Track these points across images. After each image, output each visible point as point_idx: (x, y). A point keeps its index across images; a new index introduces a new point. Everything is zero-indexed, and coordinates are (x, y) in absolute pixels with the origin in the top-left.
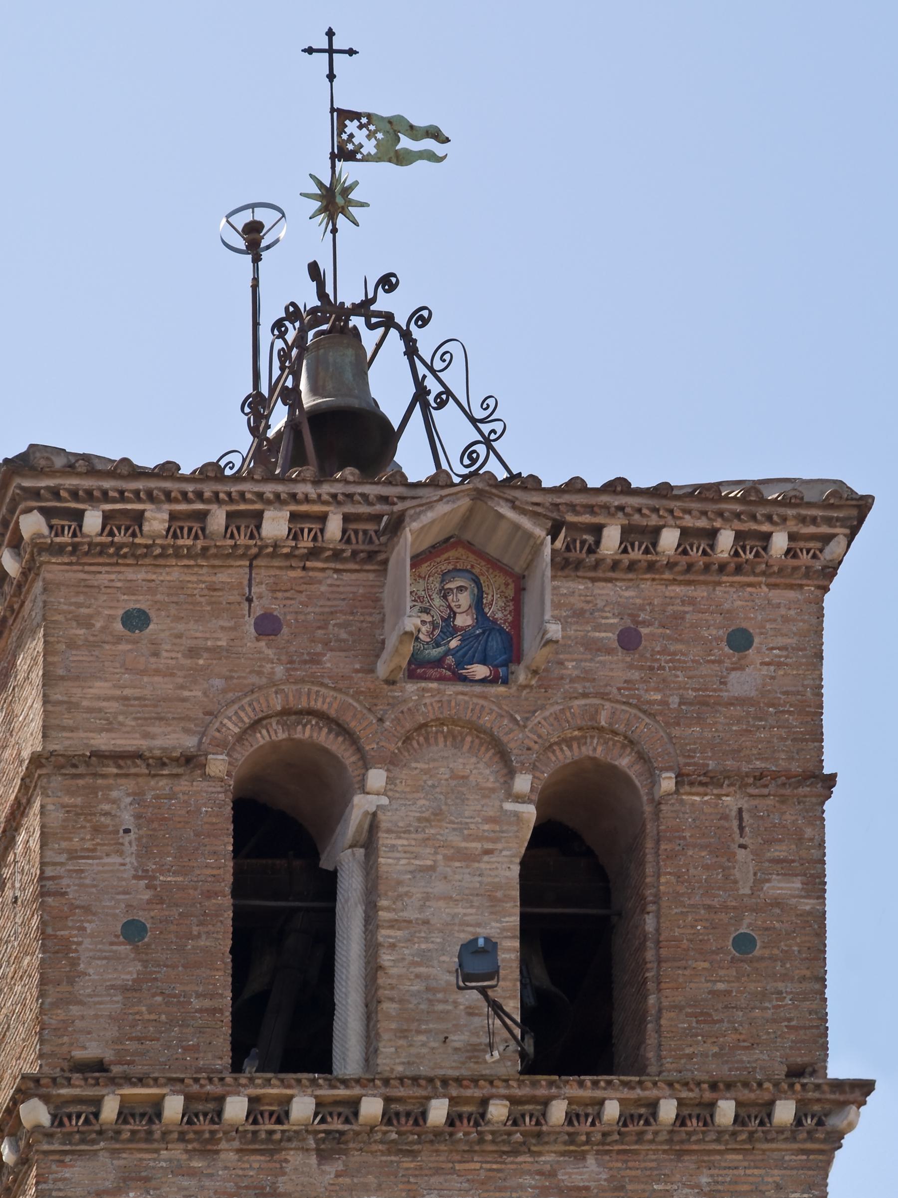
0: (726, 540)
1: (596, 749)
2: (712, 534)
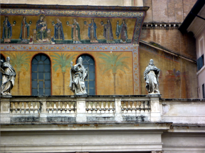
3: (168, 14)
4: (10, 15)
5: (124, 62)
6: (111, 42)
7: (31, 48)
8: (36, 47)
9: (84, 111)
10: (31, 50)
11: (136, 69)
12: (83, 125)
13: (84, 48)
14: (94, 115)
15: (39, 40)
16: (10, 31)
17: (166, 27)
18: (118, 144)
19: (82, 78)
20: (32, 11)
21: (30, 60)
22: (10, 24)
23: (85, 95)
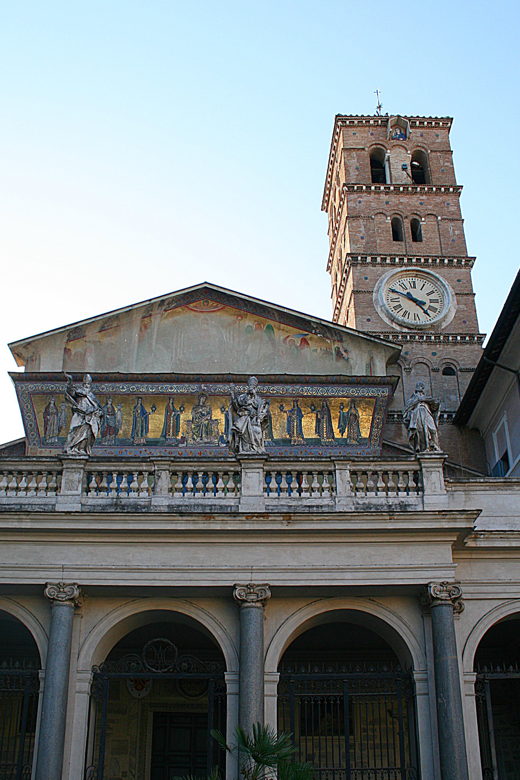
0: (433, 123)
1: (419, 148)
2: (431, 123)
12: (253, 516)
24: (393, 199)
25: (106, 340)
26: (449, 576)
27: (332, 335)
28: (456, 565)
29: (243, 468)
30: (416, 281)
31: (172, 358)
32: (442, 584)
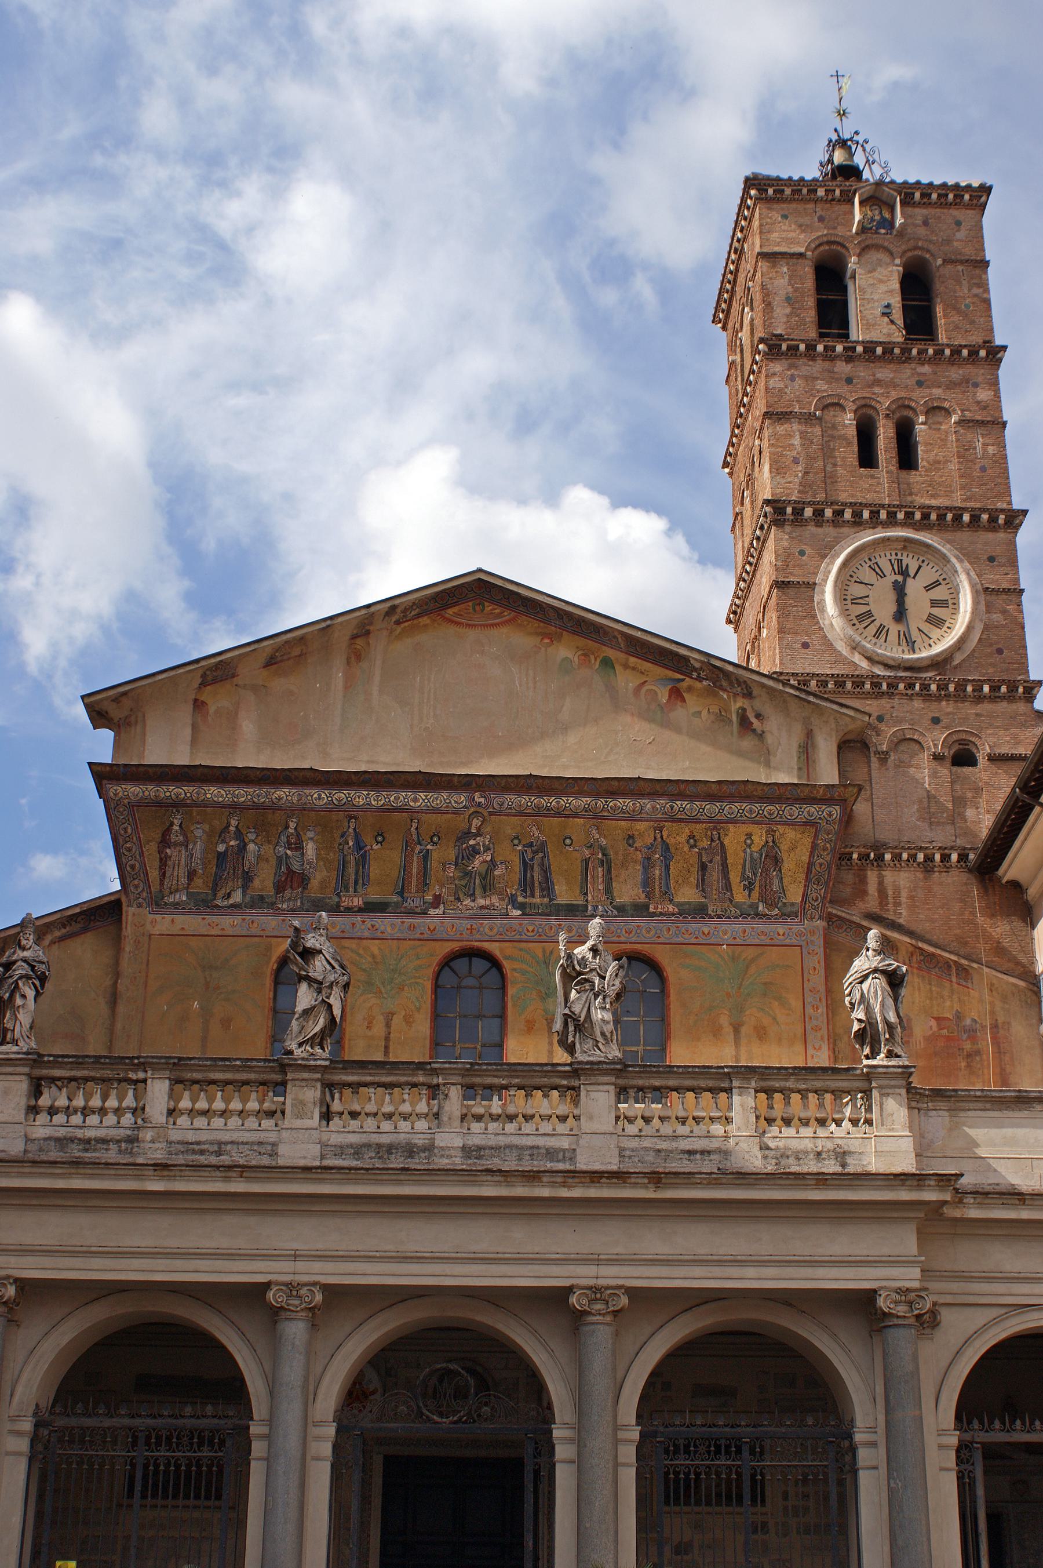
1: (918, 253)
2: (947, 195)
3: (930, 818)
4: (364, 810)
5: (771, 983)
6: (726, 910)
7: (434, 929)
8: (453, 926)
9: (606, 1123)
10: (435, 937)
11: (817, 1008)
12: (601, 1177)
13: (626, 932)
14: (647, 1143)
15: (464, 903)
16: (363, 867)
17: (925, 861)
18: (744, 1258)
19: (604, 999)
20: (441, 798)
21: (430, 972)
22: (362, 845)
23: (613, 1062)
24: (862, 372)
25: (279, 684)
26: (910, 1277)
27: (731, 684)
28: (923, 1258)
29: (583, 1084)
30: (904, 558)
31: (412, 726)
32: (899, 1291)
